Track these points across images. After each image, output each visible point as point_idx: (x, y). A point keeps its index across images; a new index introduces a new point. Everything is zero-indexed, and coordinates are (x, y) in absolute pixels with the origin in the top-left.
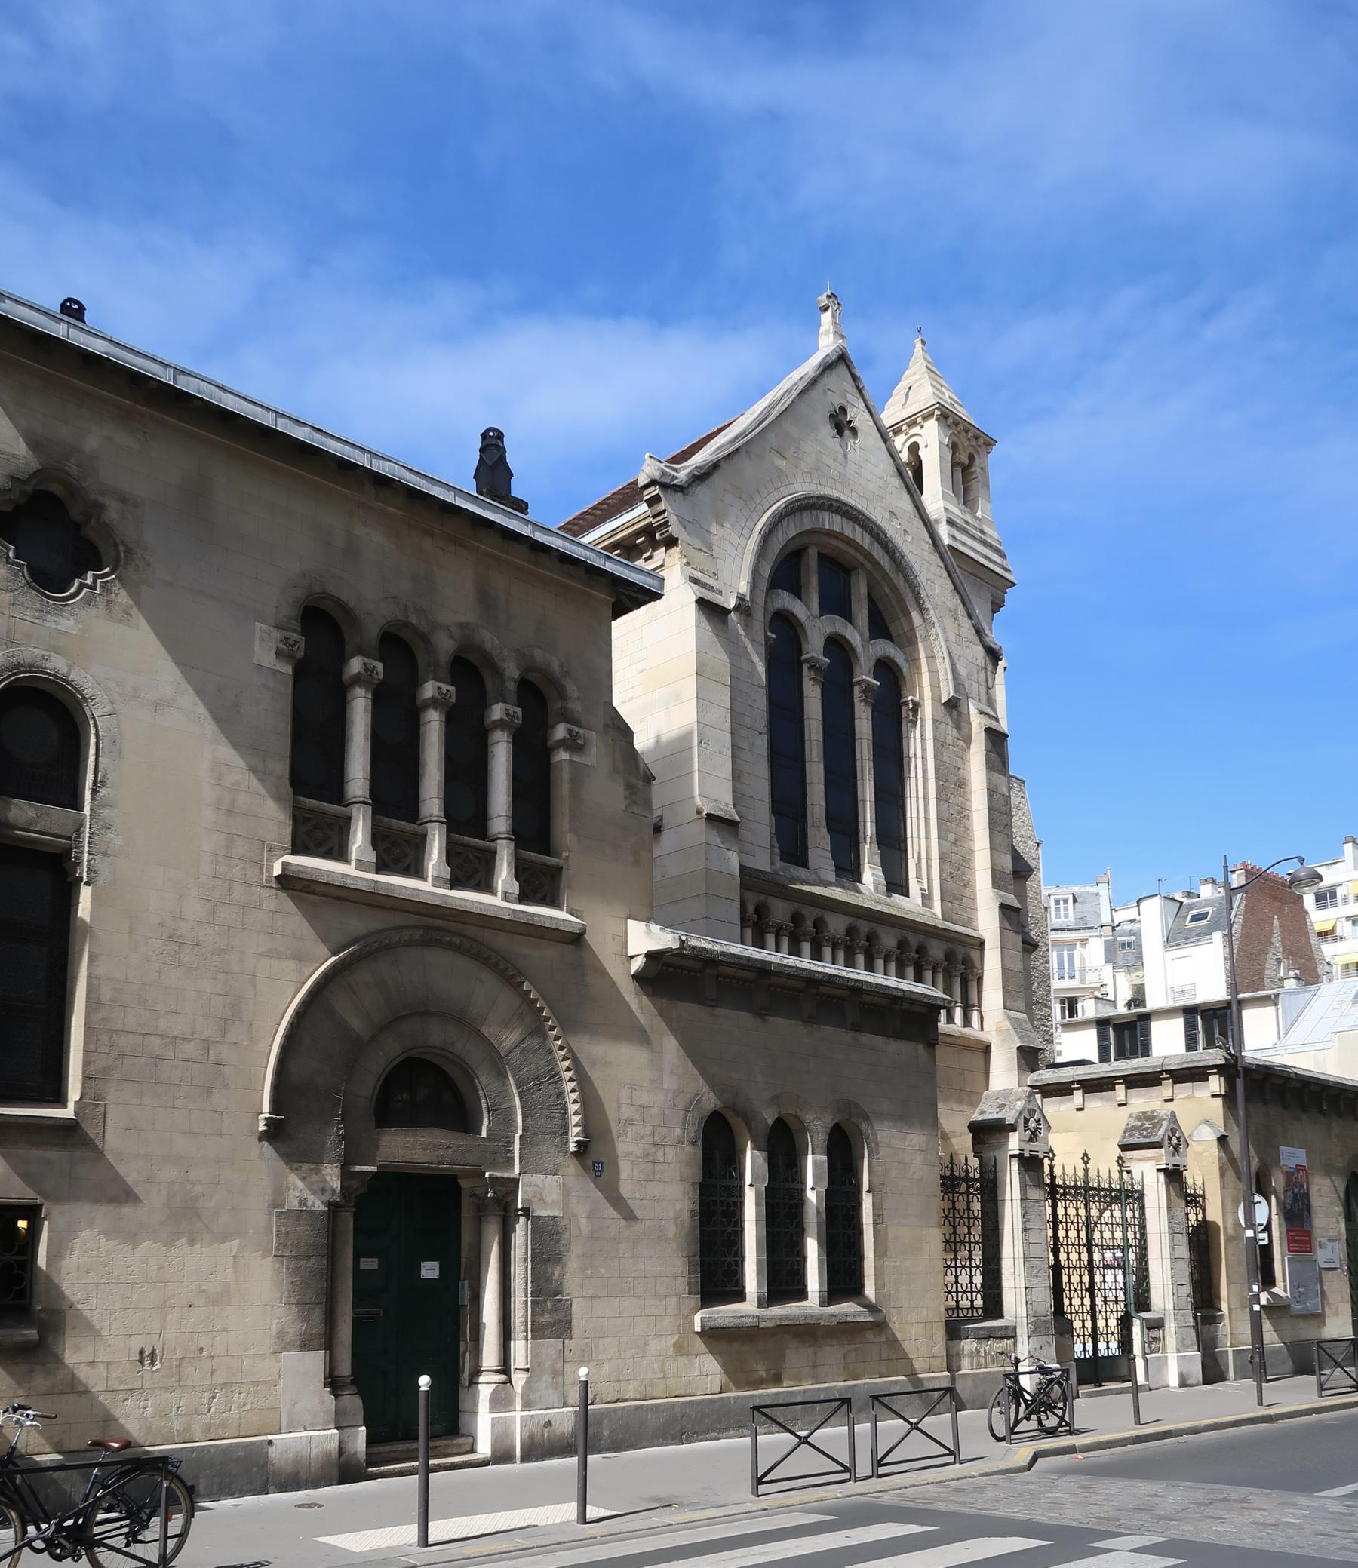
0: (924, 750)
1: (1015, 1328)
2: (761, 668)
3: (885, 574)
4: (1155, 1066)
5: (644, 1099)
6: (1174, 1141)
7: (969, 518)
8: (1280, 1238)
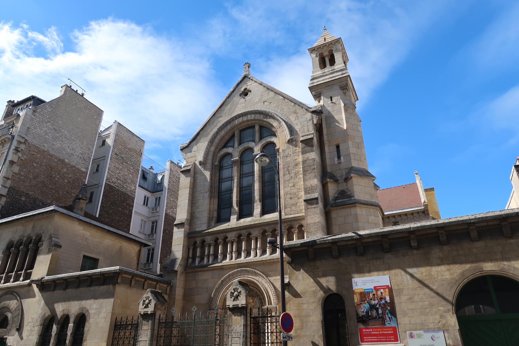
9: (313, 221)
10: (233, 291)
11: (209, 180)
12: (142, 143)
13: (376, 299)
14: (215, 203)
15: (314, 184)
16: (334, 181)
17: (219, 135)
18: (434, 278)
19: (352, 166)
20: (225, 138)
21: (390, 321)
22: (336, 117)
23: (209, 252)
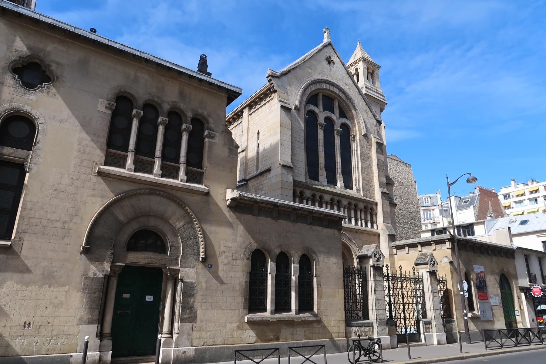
0: (357, 148)
1: (373, 323)
2: (303, 125)
3: (344, 101)
4: (429, 240)
5: (230, 245)
6: (432, 262)
7: (373, 87)
8: (475, 295)
9: (386, 210)
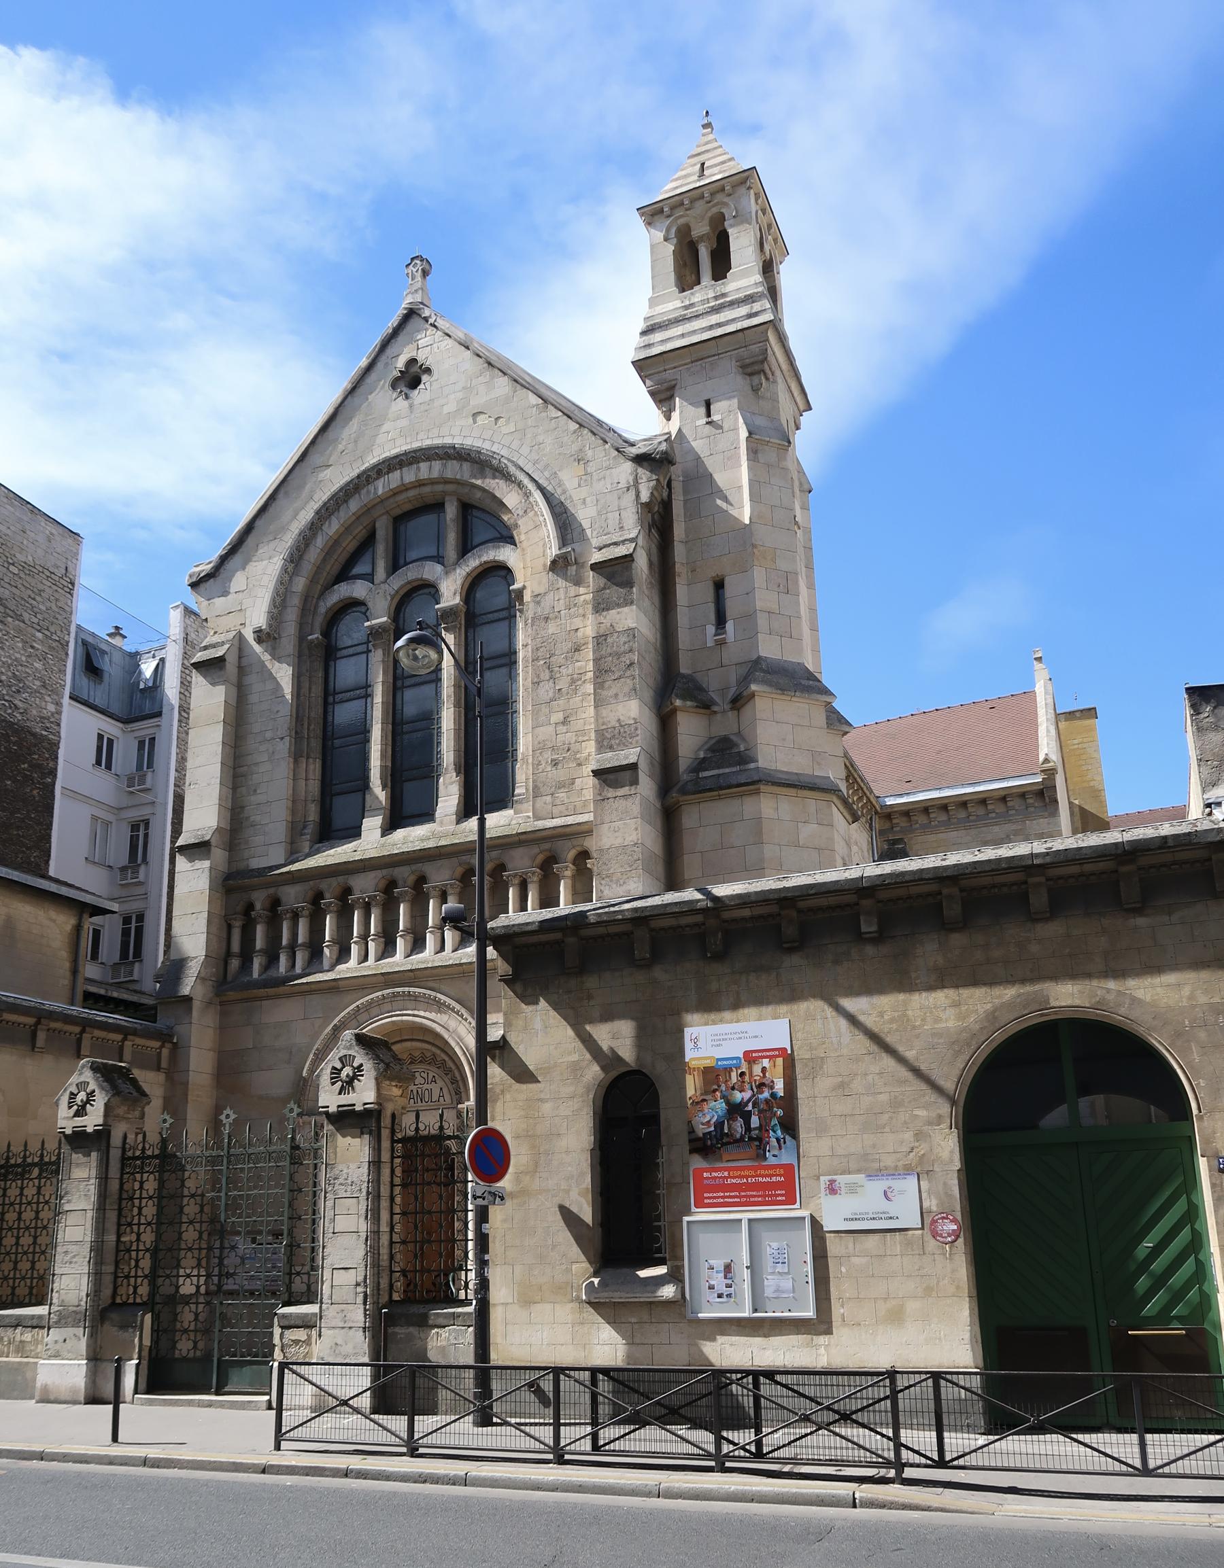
9: (618, 842)
10: (339, 1066)
11: (289, 697)
12: (70, 541)
13: (747, 1086)
14: (311, 776)
15: (629, 718)
16: (697, 707)
17: (320, 532)
18: (914, 1028)
19: (759, 658)
20: (344, 545)
21: (780, 1148)
22: (720, 478)
23: (294, 935)
